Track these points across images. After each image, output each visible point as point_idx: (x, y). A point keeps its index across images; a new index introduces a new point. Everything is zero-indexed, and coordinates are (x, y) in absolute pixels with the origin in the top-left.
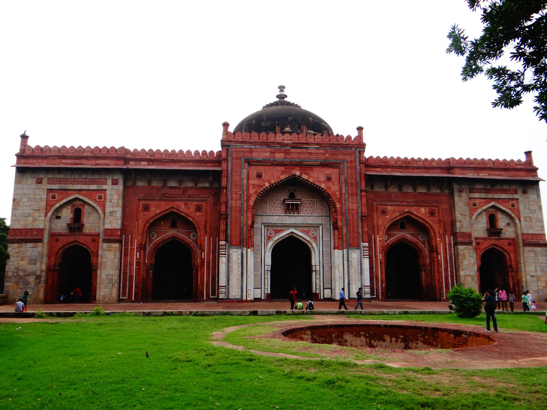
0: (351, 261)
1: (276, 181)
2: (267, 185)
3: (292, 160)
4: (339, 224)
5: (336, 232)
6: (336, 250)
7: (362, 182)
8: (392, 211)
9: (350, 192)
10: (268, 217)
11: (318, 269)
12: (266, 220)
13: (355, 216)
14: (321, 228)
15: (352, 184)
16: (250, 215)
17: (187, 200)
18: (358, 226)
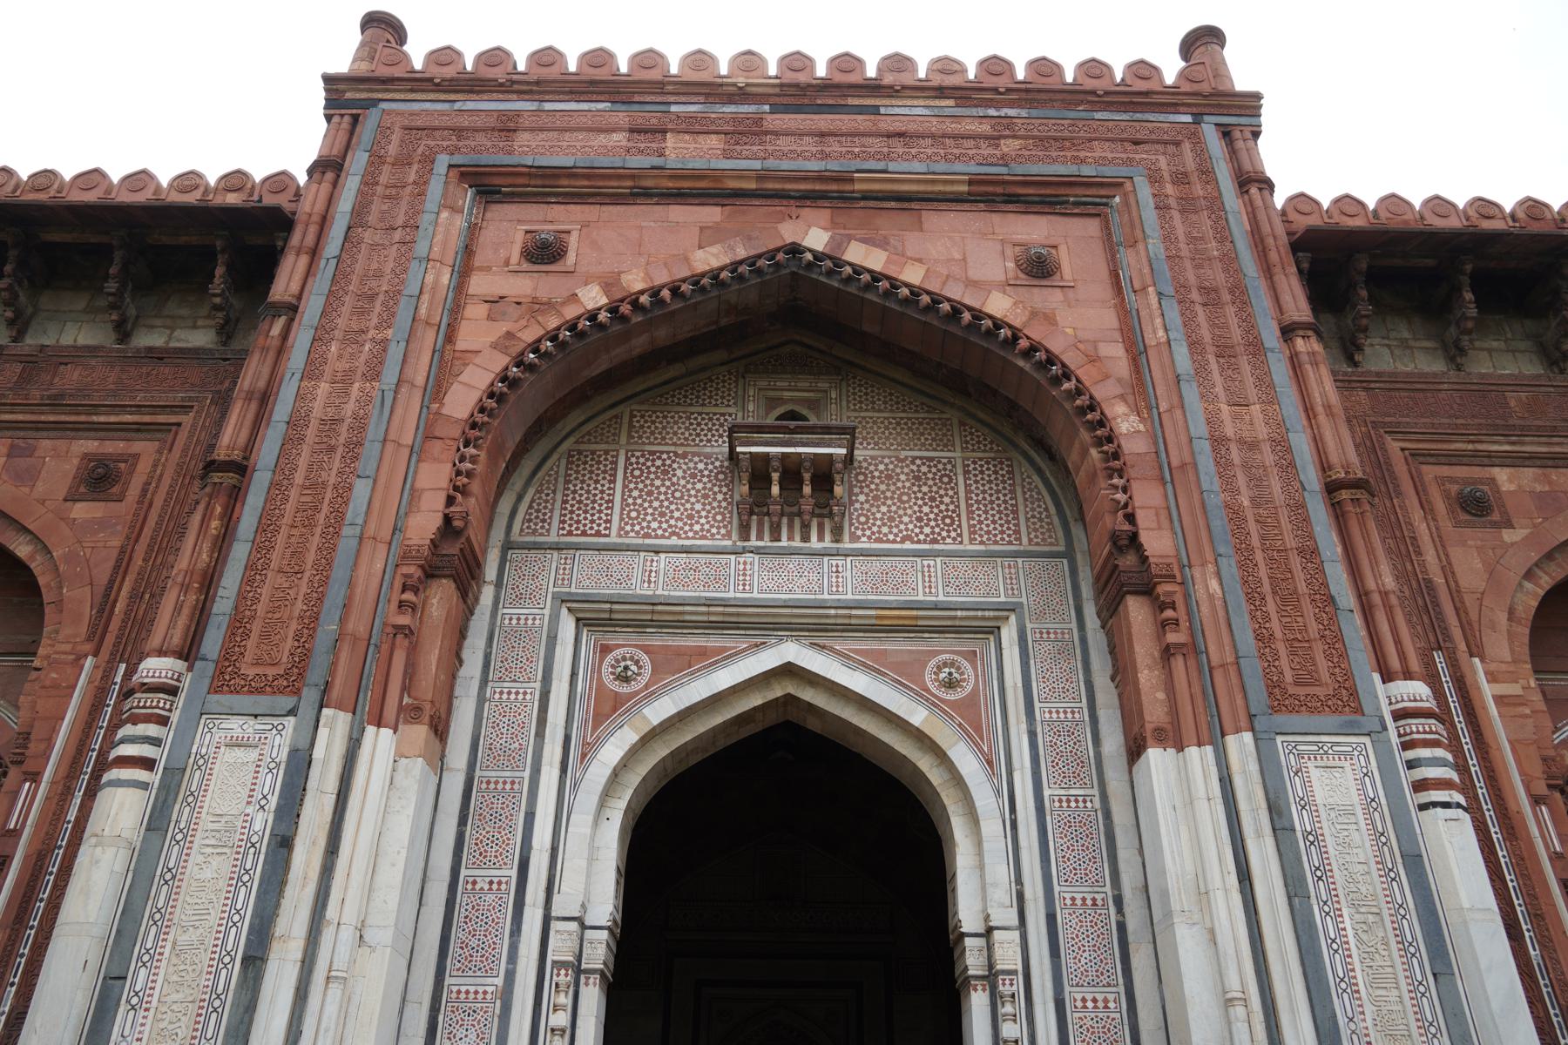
0: (1314, 838)
1: (661, 277)
2: (593, 297)
3: (771, 163)
4: (1157, 543)
5: (1137, 610)
6: (1155, 756)
7: (1280, 278)
8: (1540, 497)
9: (1206, 335)
10: (613, 559)
11: (1007, 954)
12: (593, 577)
13: (1276, 486)
14: (1009, 634)
15: (1207, 290)
16: (435, 477)
17: (38, 427)
18: (1310, 553)
